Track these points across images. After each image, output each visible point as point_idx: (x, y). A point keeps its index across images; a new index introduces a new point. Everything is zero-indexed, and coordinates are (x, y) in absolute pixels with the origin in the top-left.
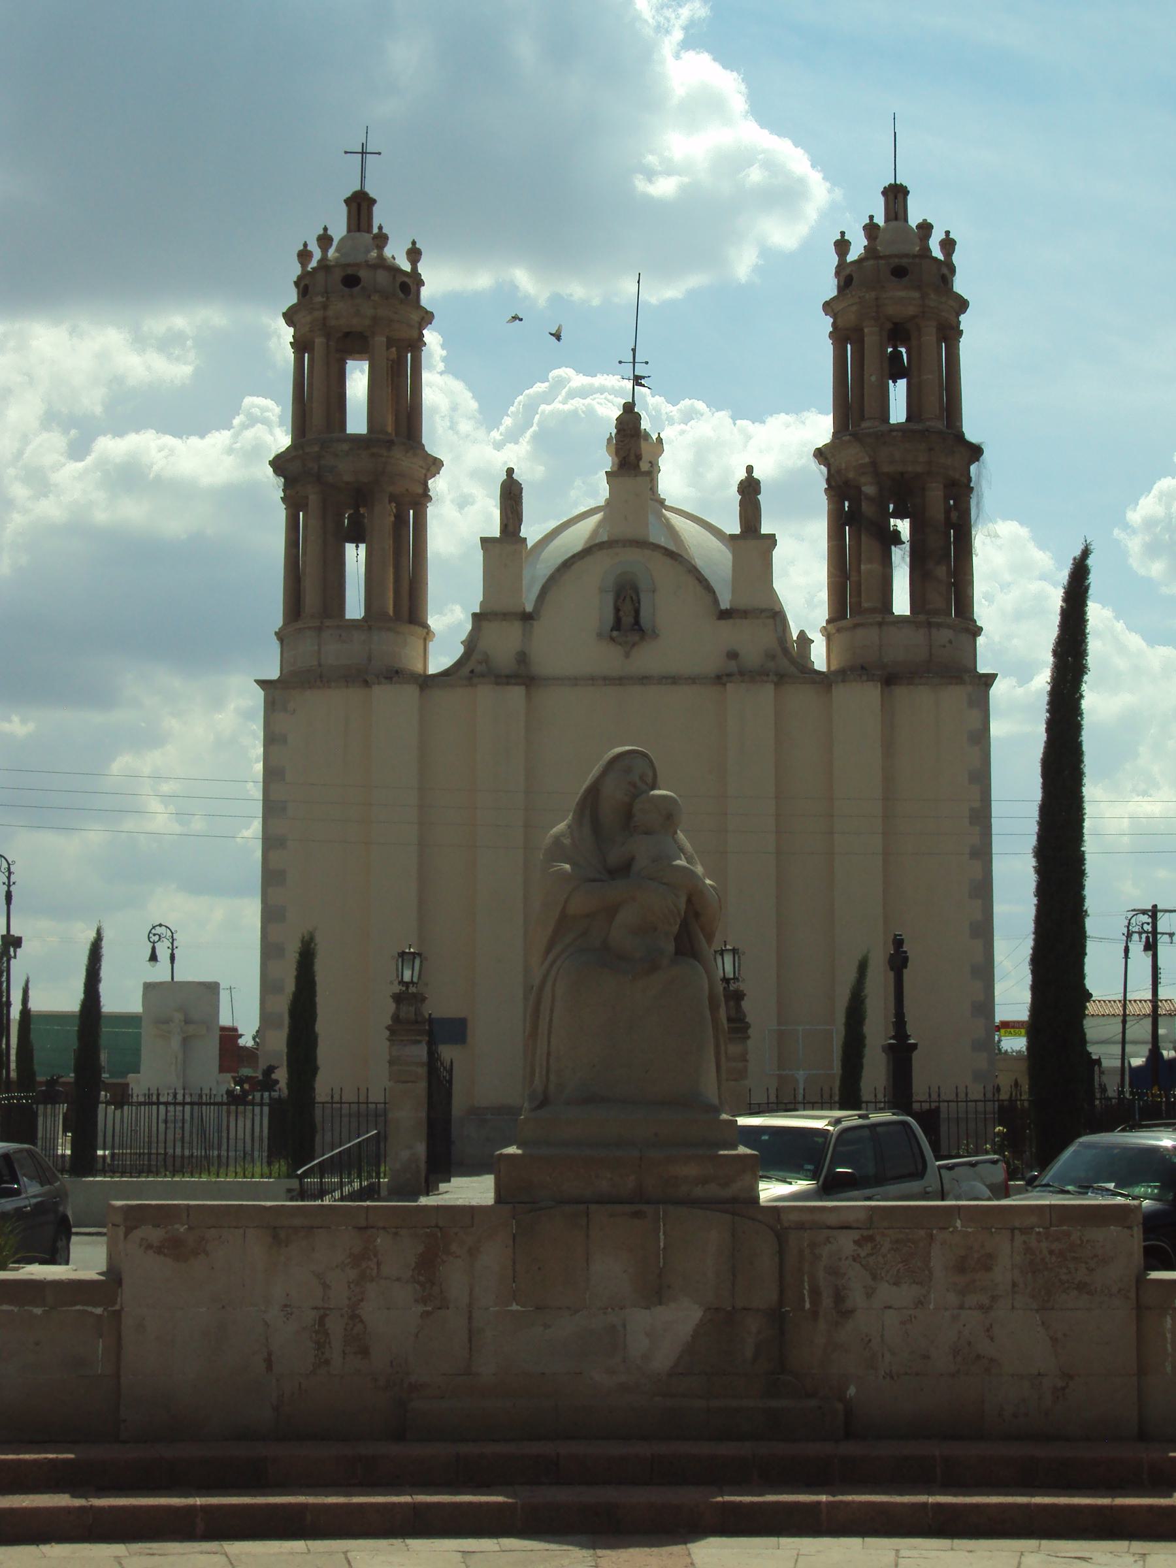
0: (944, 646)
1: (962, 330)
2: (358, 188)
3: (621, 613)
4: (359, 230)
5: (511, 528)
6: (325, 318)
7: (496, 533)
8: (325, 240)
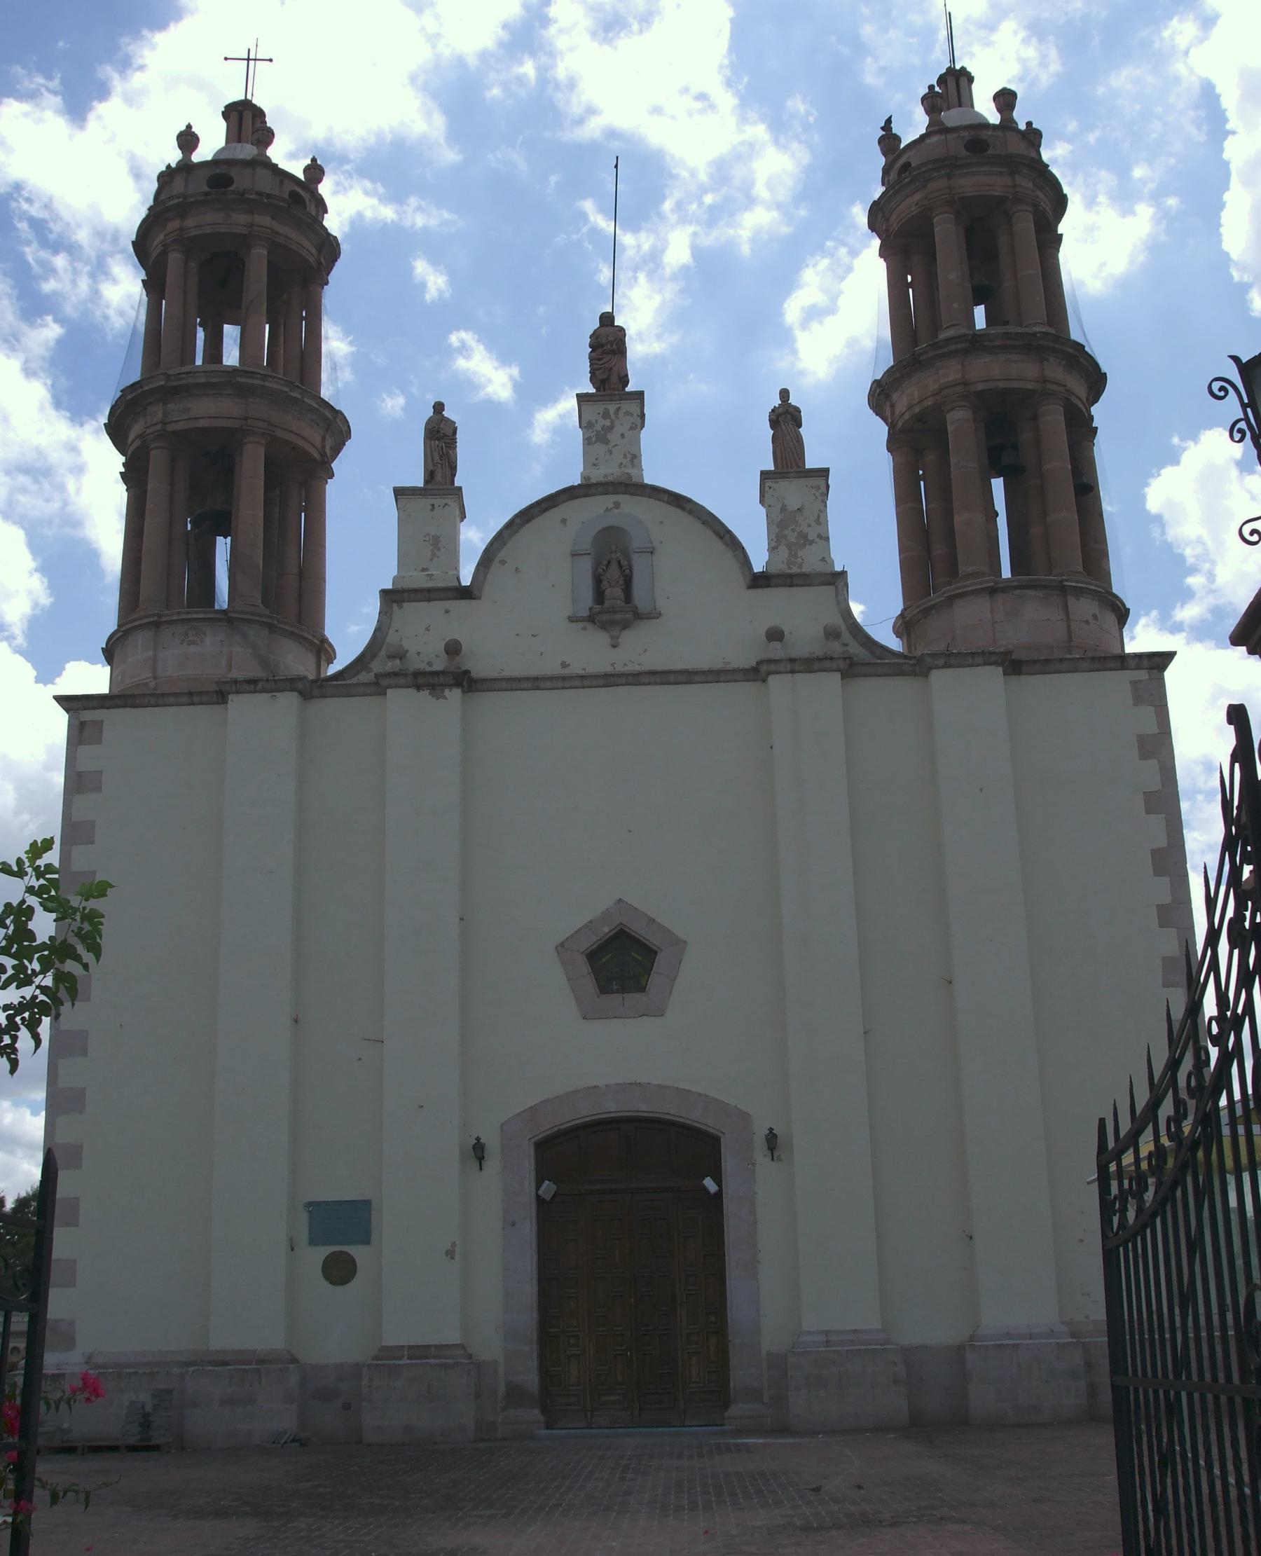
0: (1087, 622)
1: (1062, 235)
2: (243, 98)
3: (605, 583)
4: (239, 141)
5: (439, 478)
6: (181, 229)
7: (419, 482)
8: (188, 140)
